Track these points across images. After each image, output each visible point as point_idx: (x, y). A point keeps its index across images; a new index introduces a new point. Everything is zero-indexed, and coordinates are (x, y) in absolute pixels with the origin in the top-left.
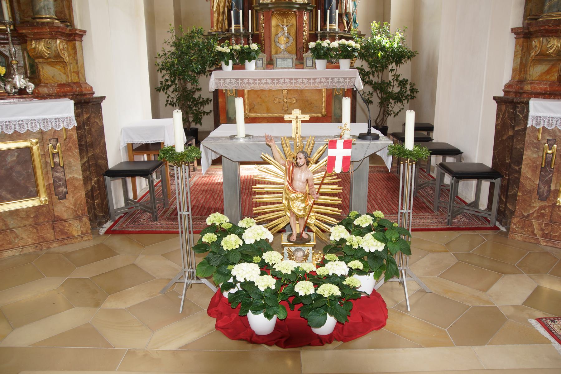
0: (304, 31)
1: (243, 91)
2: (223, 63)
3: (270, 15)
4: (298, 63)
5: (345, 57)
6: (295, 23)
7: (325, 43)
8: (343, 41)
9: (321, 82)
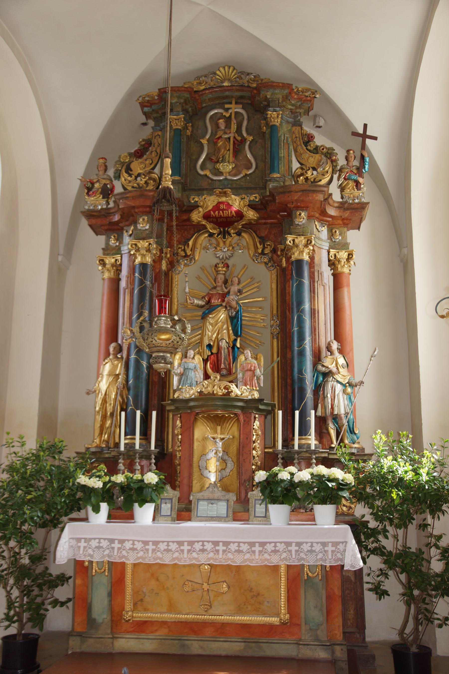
0: (254, 449)
1: (123, 565)
3: (192, 419)
4: (239, 507)
5: (323, 501)
6: (236, 434)
8: (322, 470)
9: (275, 551)
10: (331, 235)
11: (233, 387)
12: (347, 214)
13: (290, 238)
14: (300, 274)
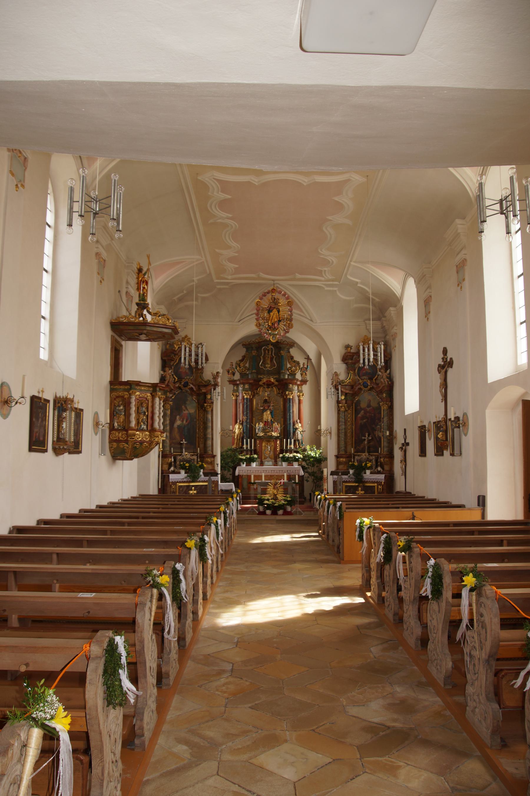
2: (242, 463)
4: (275, 463)
5: (295, 461)
7: (287, 455)
8: (295, 454)
10: (298, 388)
11: (273, 433)
12: (302, 383)
13: (287, 393)
14: (290, 402)
